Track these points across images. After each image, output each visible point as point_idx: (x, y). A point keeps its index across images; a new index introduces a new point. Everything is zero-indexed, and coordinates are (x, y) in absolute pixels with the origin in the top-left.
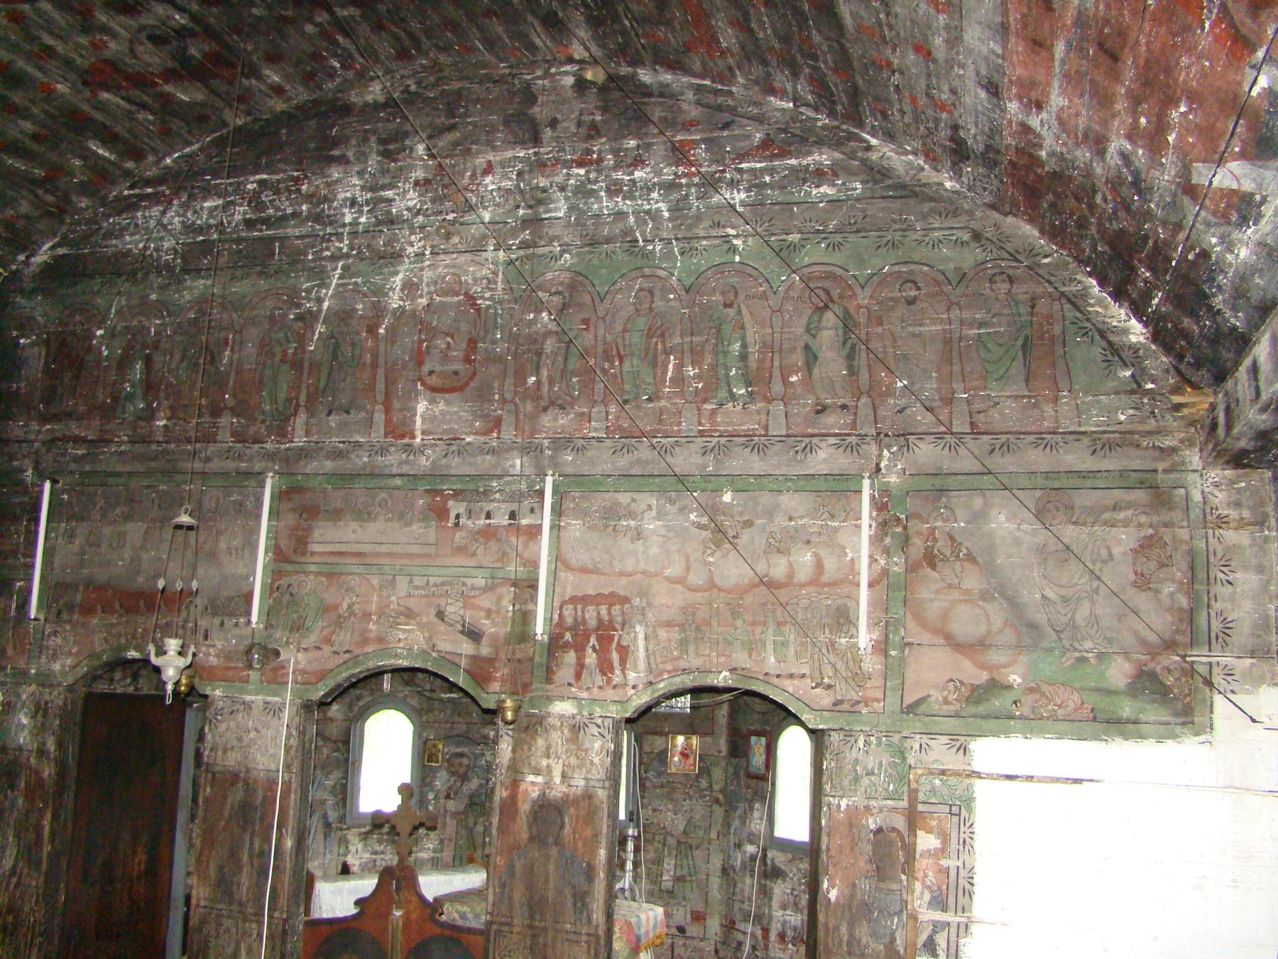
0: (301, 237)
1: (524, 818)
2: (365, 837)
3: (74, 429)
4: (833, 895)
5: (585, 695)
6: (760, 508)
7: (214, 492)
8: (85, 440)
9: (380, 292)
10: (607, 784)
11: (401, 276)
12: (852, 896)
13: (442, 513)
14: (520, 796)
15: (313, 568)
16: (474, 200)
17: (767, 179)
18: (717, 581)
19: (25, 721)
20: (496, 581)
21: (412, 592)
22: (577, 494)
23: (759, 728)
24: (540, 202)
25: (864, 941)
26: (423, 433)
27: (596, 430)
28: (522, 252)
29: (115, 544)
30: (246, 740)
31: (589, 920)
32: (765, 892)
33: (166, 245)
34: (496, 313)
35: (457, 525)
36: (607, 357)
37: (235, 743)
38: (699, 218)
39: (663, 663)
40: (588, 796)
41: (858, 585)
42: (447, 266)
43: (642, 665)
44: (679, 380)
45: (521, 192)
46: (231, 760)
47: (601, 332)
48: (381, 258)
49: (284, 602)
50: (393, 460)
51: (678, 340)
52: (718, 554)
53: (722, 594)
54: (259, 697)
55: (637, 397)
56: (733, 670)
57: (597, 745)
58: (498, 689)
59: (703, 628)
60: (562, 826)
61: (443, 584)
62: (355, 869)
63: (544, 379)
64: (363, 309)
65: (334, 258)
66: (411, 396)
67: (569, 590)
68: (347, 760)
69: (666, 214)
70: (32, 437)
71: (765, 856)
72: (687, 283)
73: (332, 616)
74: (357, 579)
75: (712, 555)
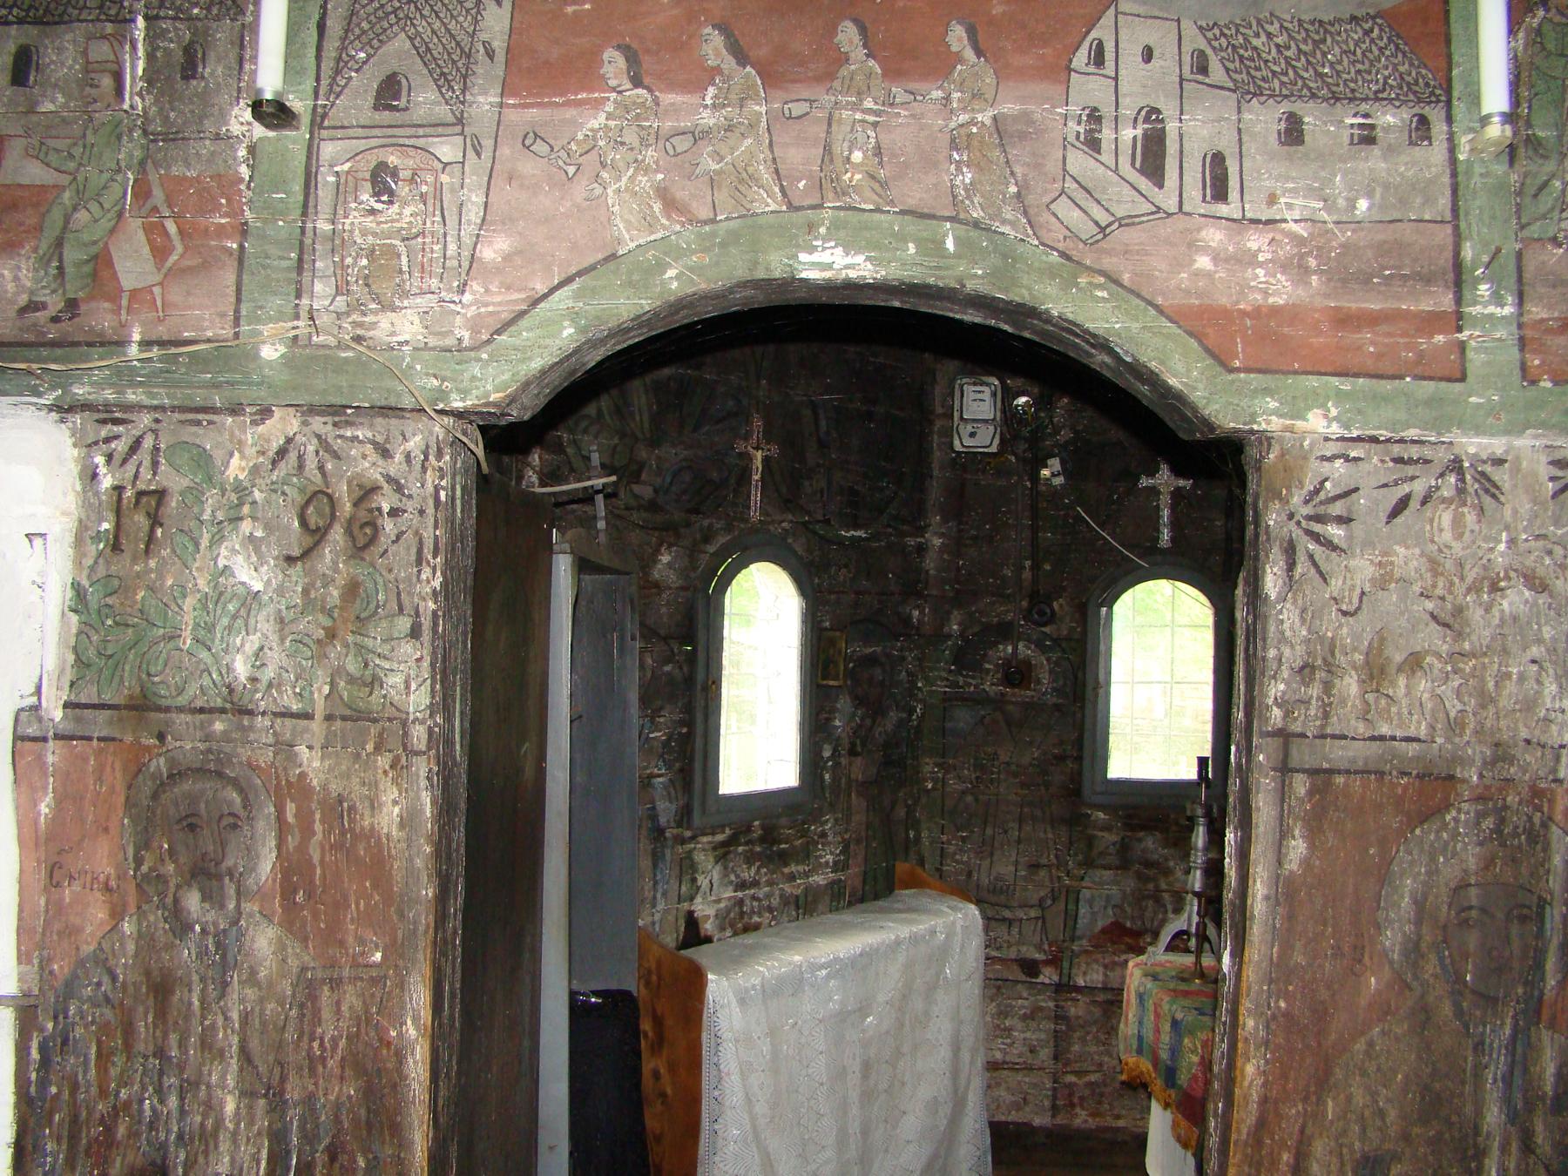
2: (723, 852)
19: (249, 575)
30: (1481, 627)
37: (1433, 639)
54: (1527, 443)
62: (708, 927)
68: (690, 680)
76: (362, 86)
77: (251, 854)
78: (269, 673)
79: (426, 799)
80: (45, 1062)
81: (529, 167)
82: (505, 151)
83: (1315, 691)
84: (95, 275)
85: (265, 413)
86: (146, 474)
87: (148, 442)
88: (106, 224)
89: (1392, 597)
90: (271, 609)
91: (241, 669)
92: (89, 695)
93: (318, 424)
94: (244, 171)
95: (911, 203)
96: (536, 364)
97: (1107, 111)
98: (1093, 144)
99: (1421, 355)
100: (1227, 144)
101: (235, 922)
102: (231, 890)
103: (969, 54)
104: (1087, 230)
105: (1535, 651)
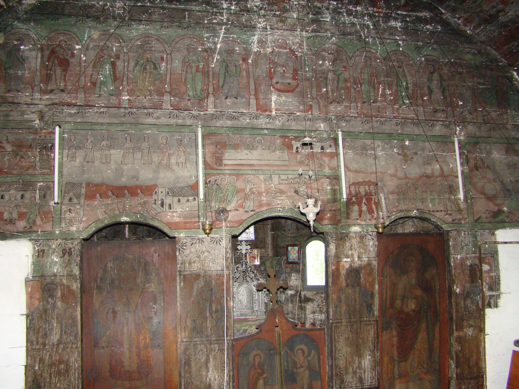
0: (199, 11)
1: (343, 277)
3: (66, 98)
4: (458, 291)
5: (363, 223)
6: (419, 148)
7: (163, 134)
8: (75, 105)
9: (248, 43)
10: (376, 258)
11: (256, 37)
12: (464, 290)
13: (290, 147)
14: (341, 268)
15: (227, 172)
16: (288, 7)
17: (408, 19)
18: (408, 175)
19: (56, 259)
20: (320, 177)
21: (281, 182)
22: (349, 140)
23: (292, 243)
24: (318, 13)
25: (469, 306)
26: (276, 110)
27: (353, 113)
28: (313, 34)
29: (104, 161)
30: (202, 257)
31: (374, 315)
32: (302, 309)
33: (118, 5)
34: (305, 59)
35: (297, 152)
36: (355, 83)
37: (196, 259)
38: (385, 30)
39: (392, 208)
40: (369, 264)
41: (457, 177)
42: (279, 35)
43: (384, 210)
44: (384, 95)
45: (309, 7)
46: (195, 267)
47: (351, 73)
48: (246, 27)
49: (214, 188)
50: (262, 122)
51: (382, 79)
52: (406, 165)
53: (411, 181)
55: (369, 101)
56: (418, 210)
57: (371, 243)
58: (326, 223)
59: (405, 194)
60: (360, 278)
61: (295, 178)
63: (329, 90)
64: (239, 50)
65: (220, 24)
66: (268, 93)
67: (351, 180)
69: (372, 27)
70: (36, 102)
71: (300, 294)
72: (384, 56)
73: (242, 194)
74: (252, 176)
75: (404, 165)
76: (67, 199)
77: (57, 293)
78: (59, 271)
79: (79, 285)
80: (30, 322)
81: (88, 209)
82: (85, 207)
83: (183, 266)
84: (34, 223)
85: (57, 240)
86: (42, 248)
87: (42, 244)
88: (35, 217)
89: (192, 254)
90: (59, 263)
91: (55, 271)
92: (35, 275)
93: (64, 241)
94: (53, 210)
95: (134, 212)
96: (90, 233)
97: (157, 199)
98: (155, 203)
99: (194, 226)
100: (171, 203)
101: (55, 302)
102: (55, 297)
103: (141, 193)
104: (155, 214)
105: (209, 260)
